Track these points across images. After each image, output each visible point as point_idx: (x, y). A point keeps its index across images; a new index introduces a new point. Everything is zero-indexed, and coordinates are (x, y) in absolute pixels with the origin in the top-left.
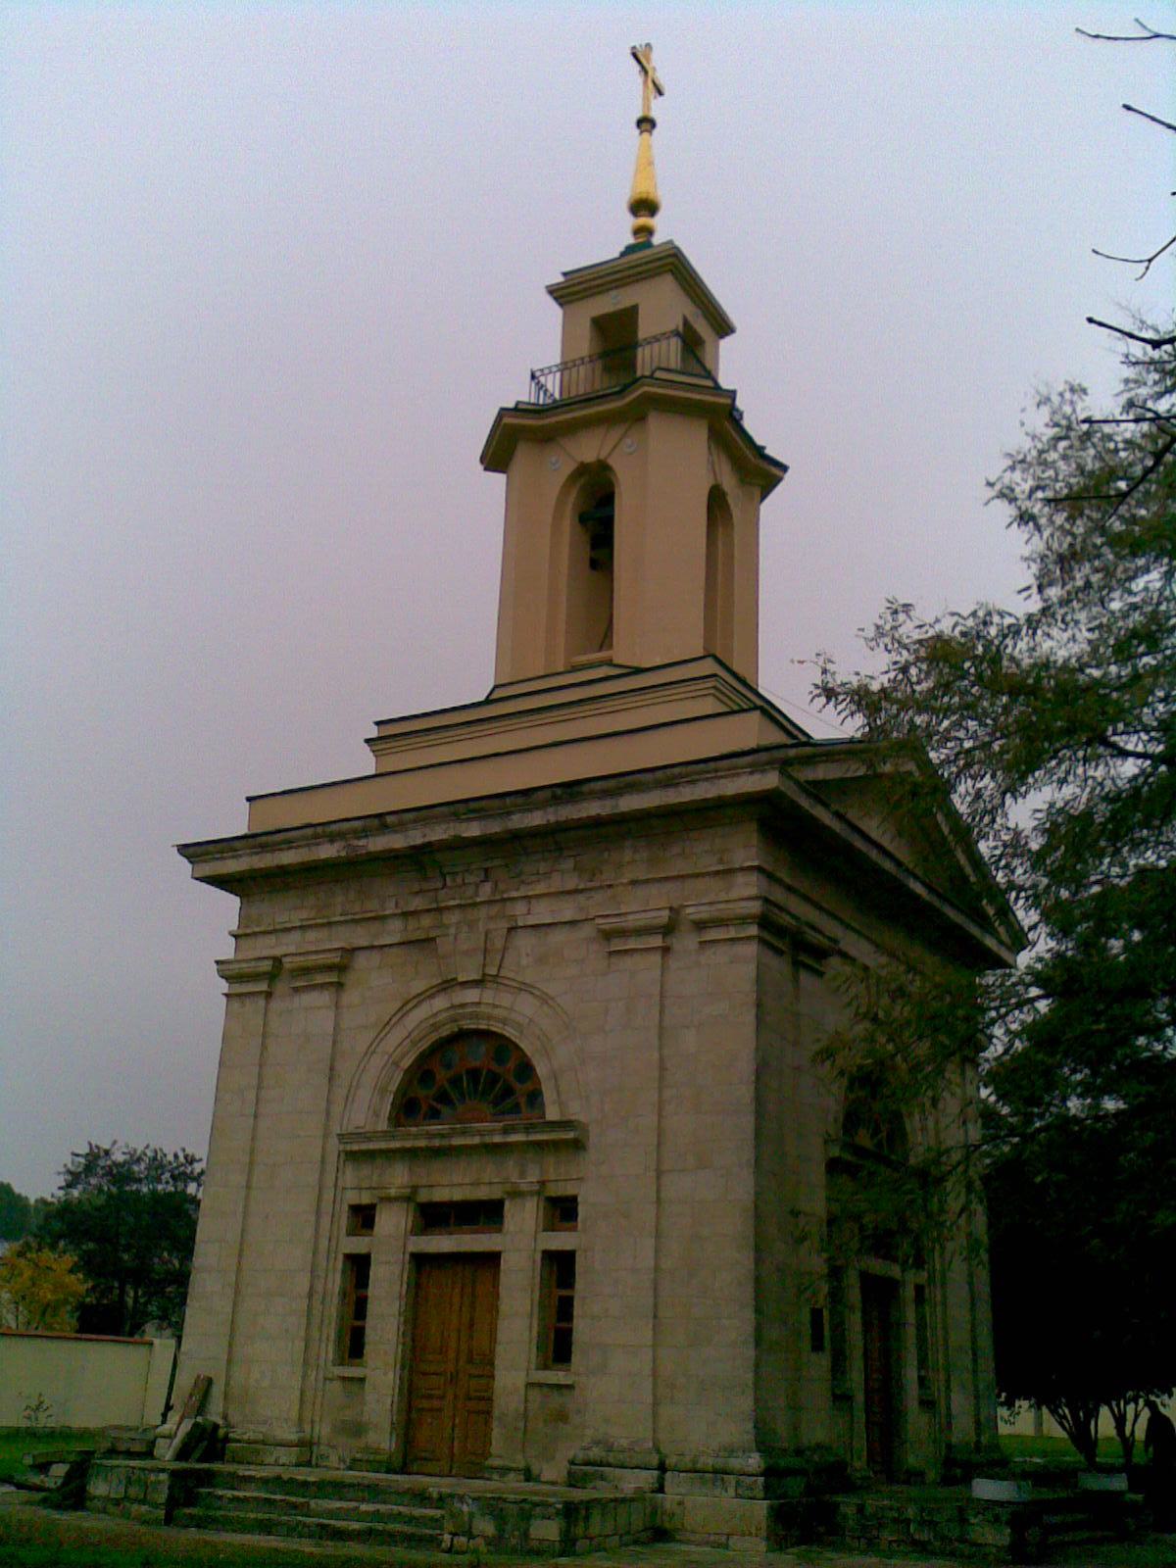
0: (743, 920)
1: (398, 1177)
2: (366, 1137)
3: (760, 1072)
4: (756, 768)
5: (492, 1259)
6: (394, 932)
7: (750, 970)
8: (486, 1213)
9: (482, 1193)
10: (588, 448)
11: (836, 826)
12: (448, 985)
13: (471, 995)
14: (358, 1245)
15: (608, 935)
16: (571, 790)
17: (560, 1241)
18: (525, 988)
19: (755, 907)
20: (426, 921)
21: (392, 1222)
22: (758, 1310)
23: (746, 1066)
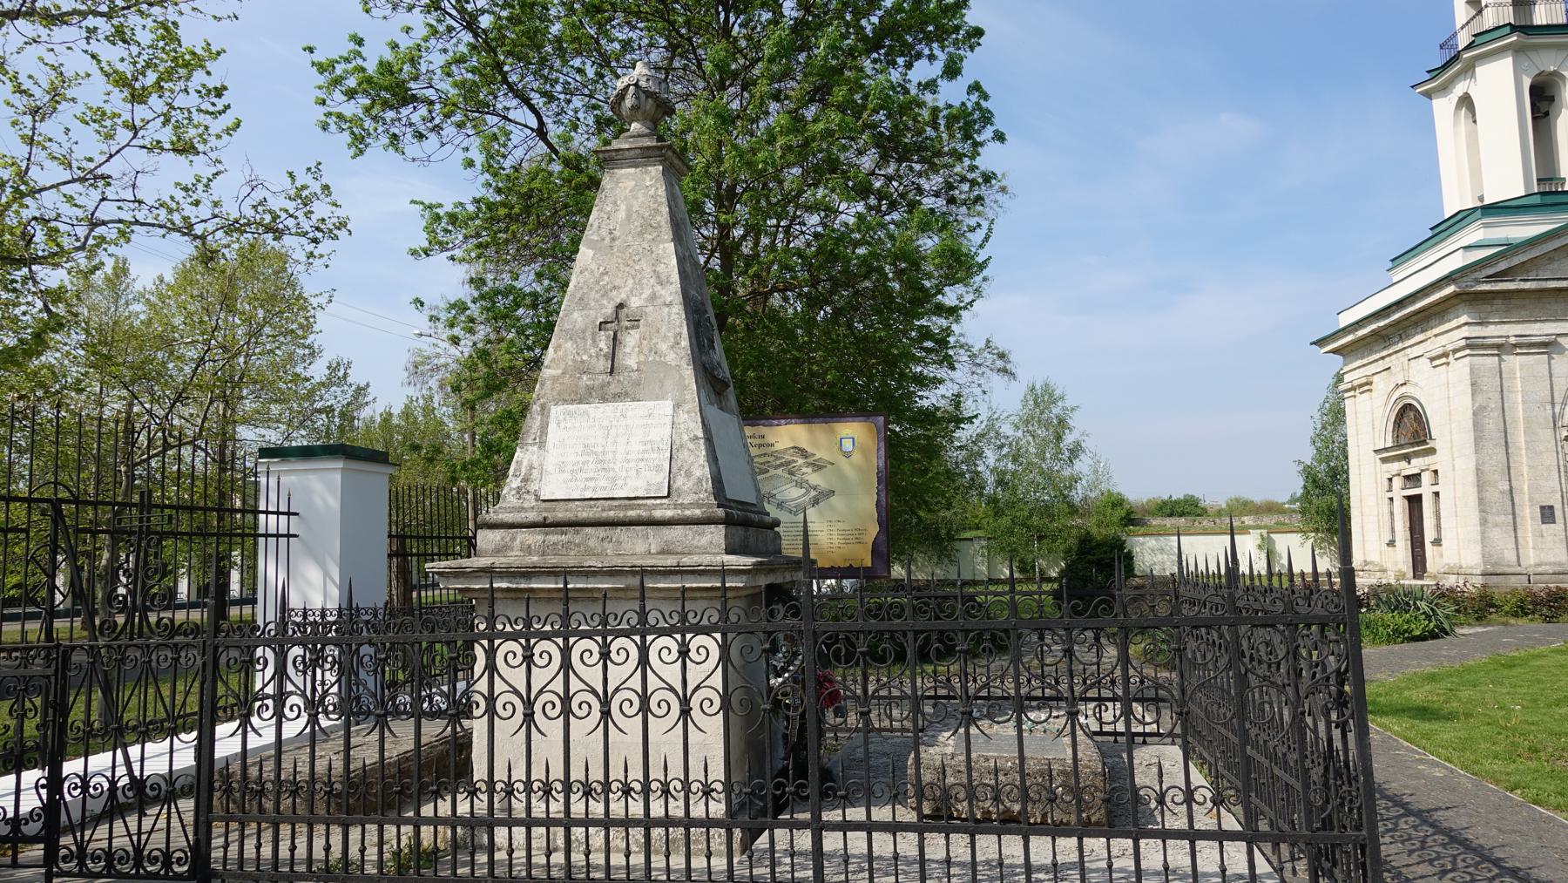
0: (1463, 348)
1: (1395, 467)
2: (1386, 450)
3: (1475, 414)
4: (1448, 285)
5: (1418, 498)
6: (1381, 365)
7: (1467, 370)
8: (1414, 479)
9: (1416, 471)
10: (1459, 89)
11: (1527, 285)
12: (1398, 386)
13: (1403, 390)
14: (1390, 495)
15: (1432, 359)
16: (1400, 304)
17: (1435, 489)
18: (1416, 385)
19: (1463, 343)
20: (1387, 359)
21: (1397, 482)
22: (1482, 511)
23: (1470, 412)
